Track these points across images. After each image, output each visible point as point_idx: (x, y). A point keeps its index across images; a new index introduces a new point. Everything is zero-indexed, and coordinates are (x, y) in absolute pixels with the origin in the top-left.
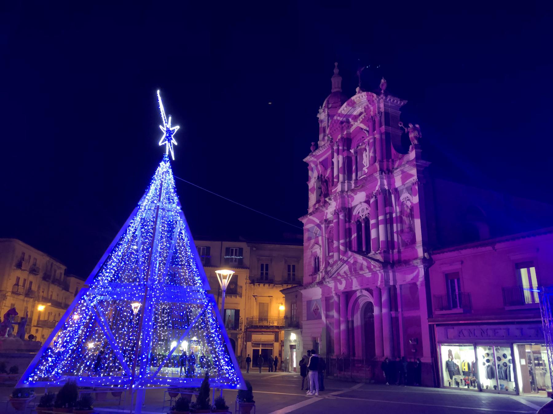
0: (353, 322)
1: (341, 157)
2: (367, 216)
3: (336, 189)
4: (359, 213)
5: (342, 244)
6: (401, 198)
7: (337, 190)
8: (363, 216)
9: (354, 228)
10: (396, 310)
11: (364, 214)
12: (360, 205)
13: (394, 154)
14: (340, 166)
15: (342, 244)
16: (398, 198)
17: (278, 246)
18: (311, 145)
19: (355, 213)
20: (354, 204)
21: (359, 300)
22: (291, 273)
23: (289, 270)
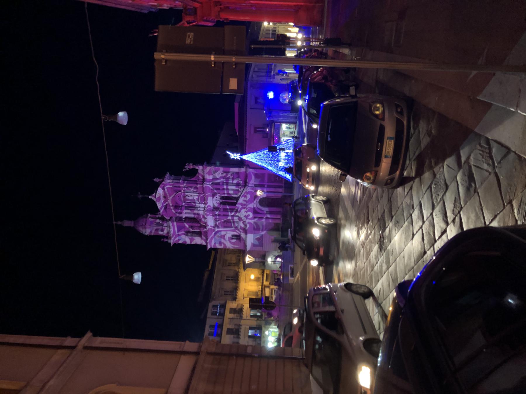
0: (267, 211)
1: (185, 211)
2: (220, 198)
3: (201, 215)
4: (217, 203)
5: (231, 213)
6: (218, 177)
7: (202, 215)
8: (219, 200)
9: (224, 207)
10: (264, 185)
11: (218, 199)
12: (214, 202)
13: (195, 178)
14: (189, 211)
15: (231, 213)
16: (217, 179)
17: (214, 284)
18: (163, 241)
19: (216, 205)
20: (212, 206)
21: (258, 207)
22: (230, 278)
23: (229, 280)
